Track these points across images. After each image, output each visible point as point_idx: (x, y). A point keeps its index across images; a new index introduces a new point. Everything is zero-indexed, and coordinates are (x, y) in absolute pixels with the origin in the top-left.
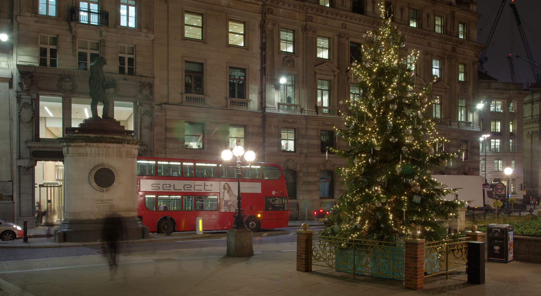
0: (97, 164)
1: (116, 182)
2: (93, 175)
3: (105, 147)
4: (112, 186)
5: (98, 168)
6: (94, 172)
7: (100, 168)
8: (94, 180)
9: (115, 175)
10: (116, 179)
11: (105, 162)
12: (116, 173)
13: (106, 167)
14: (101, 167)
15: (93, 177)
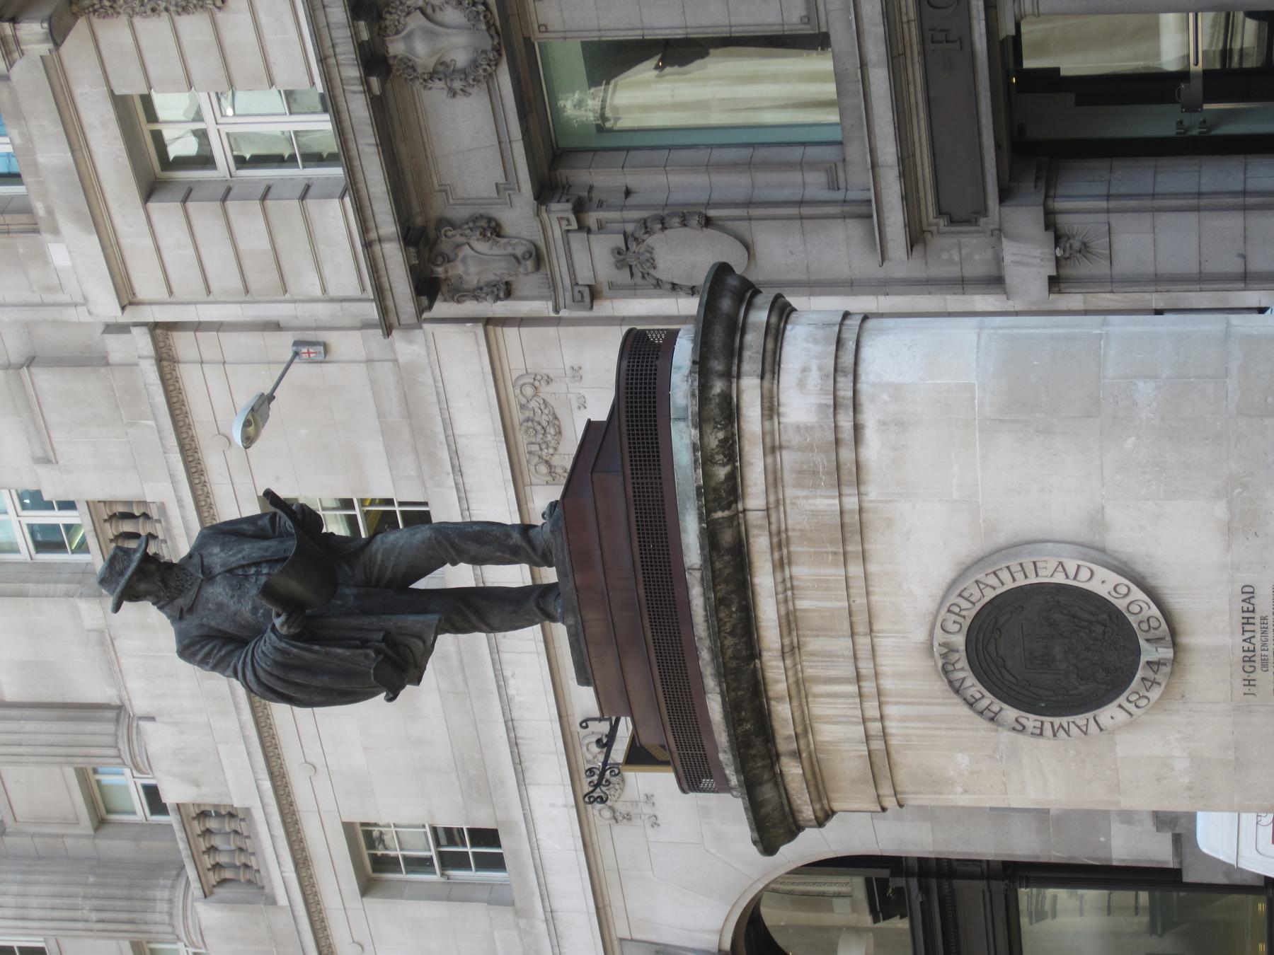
0: (940, 685)
1: (1084, 574)
2: (1031, 721)
3: (791, 650)
4: (1121, 604)
5: (974, 687)
6: (1010, 713)
7: (971, 680)
8: (1080, 719)
9: (1021, 581)
10: (1060, 579)
11: (920, 635)
12: (1005, 575)
13: (959, 640)
14: (964, 673)
15: (1047, 719)
